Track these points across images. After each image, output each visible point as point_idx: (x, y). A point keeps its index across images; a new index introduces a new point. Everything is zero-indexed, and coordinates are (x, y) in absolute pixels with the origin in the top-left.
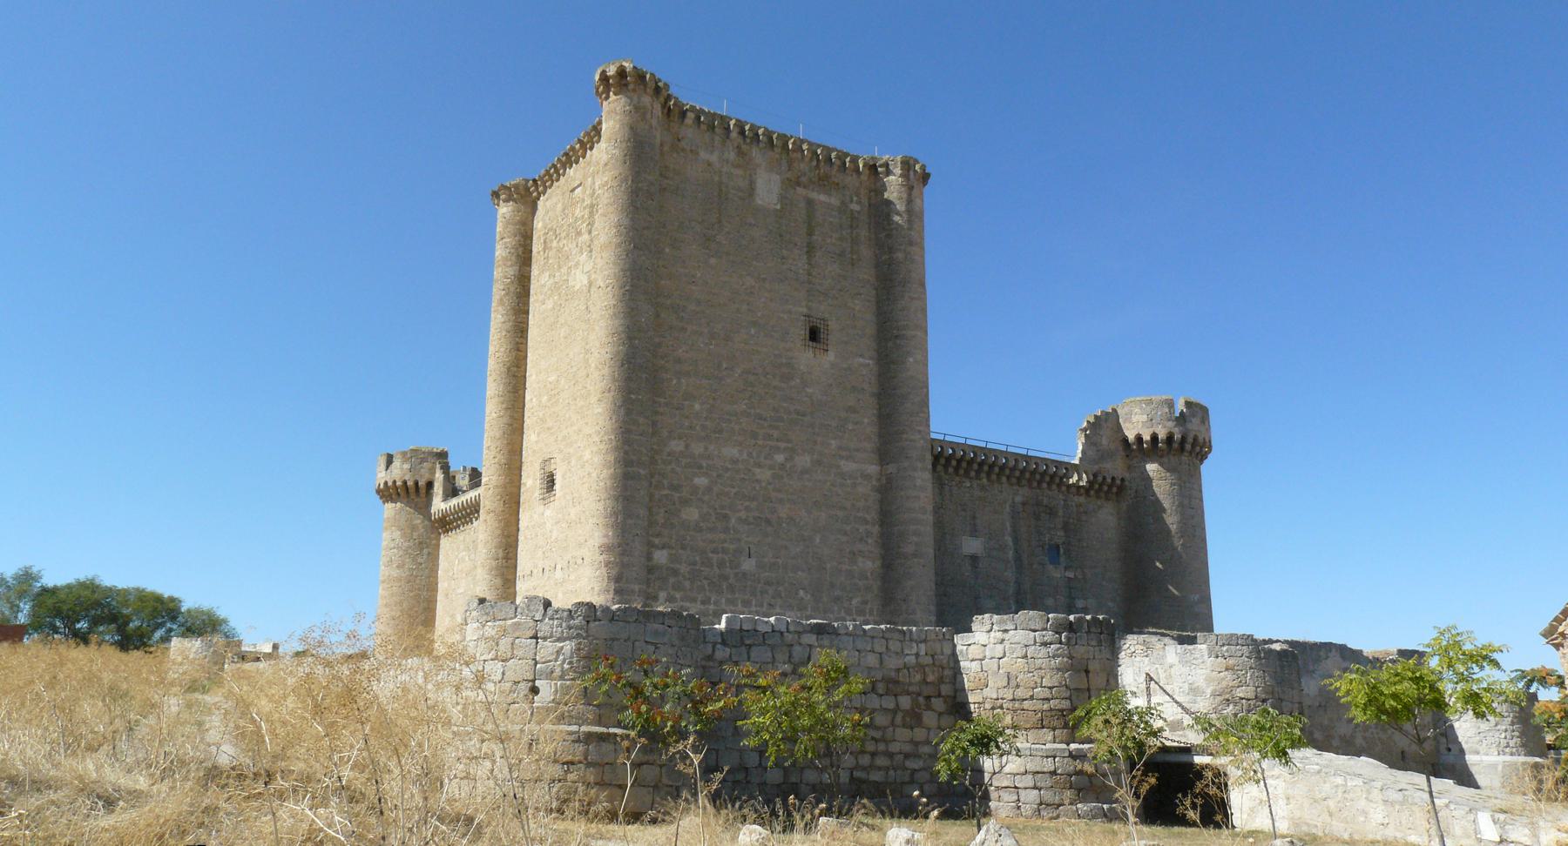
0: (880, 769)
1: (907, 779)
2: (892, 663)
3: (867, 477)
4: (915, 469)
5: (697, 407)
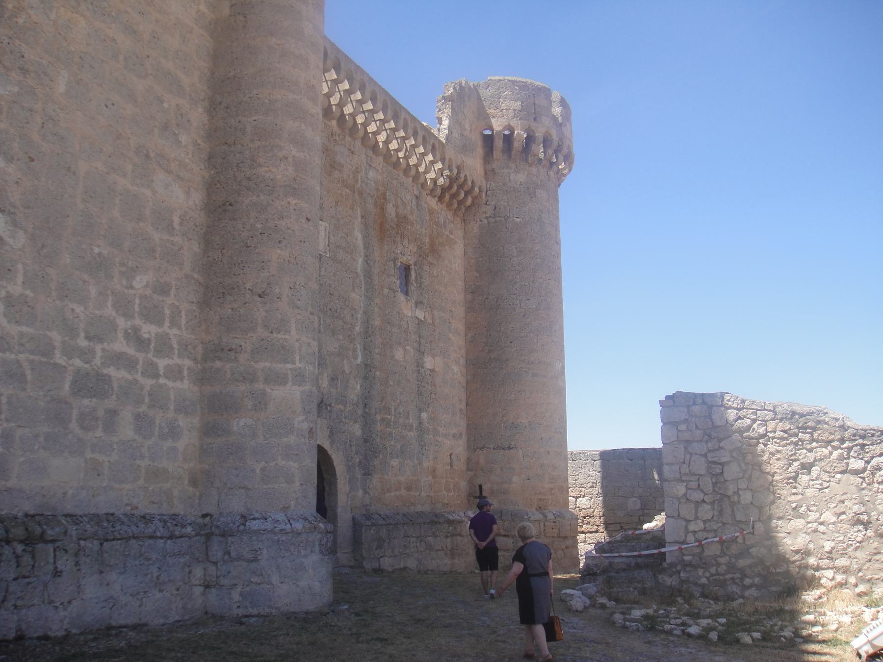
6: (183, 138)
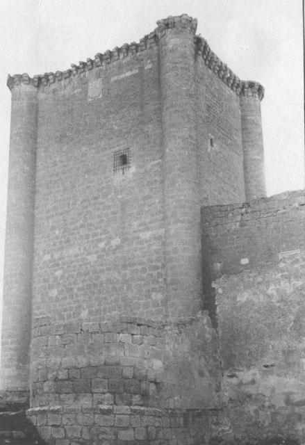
5: (57, 232)
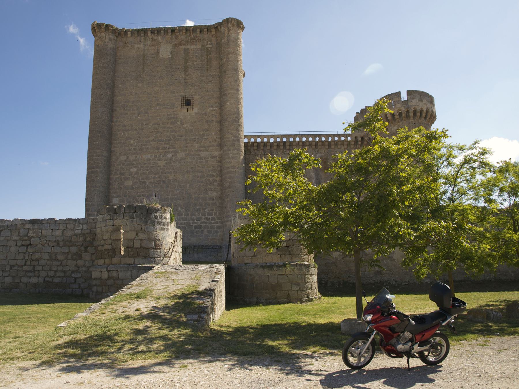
0: (59, 277)
1: (72, 281)
2: (69, 233)
3: (213, 157)
4: (229, 150)
5: (132, 142)
6: (215, 184)
